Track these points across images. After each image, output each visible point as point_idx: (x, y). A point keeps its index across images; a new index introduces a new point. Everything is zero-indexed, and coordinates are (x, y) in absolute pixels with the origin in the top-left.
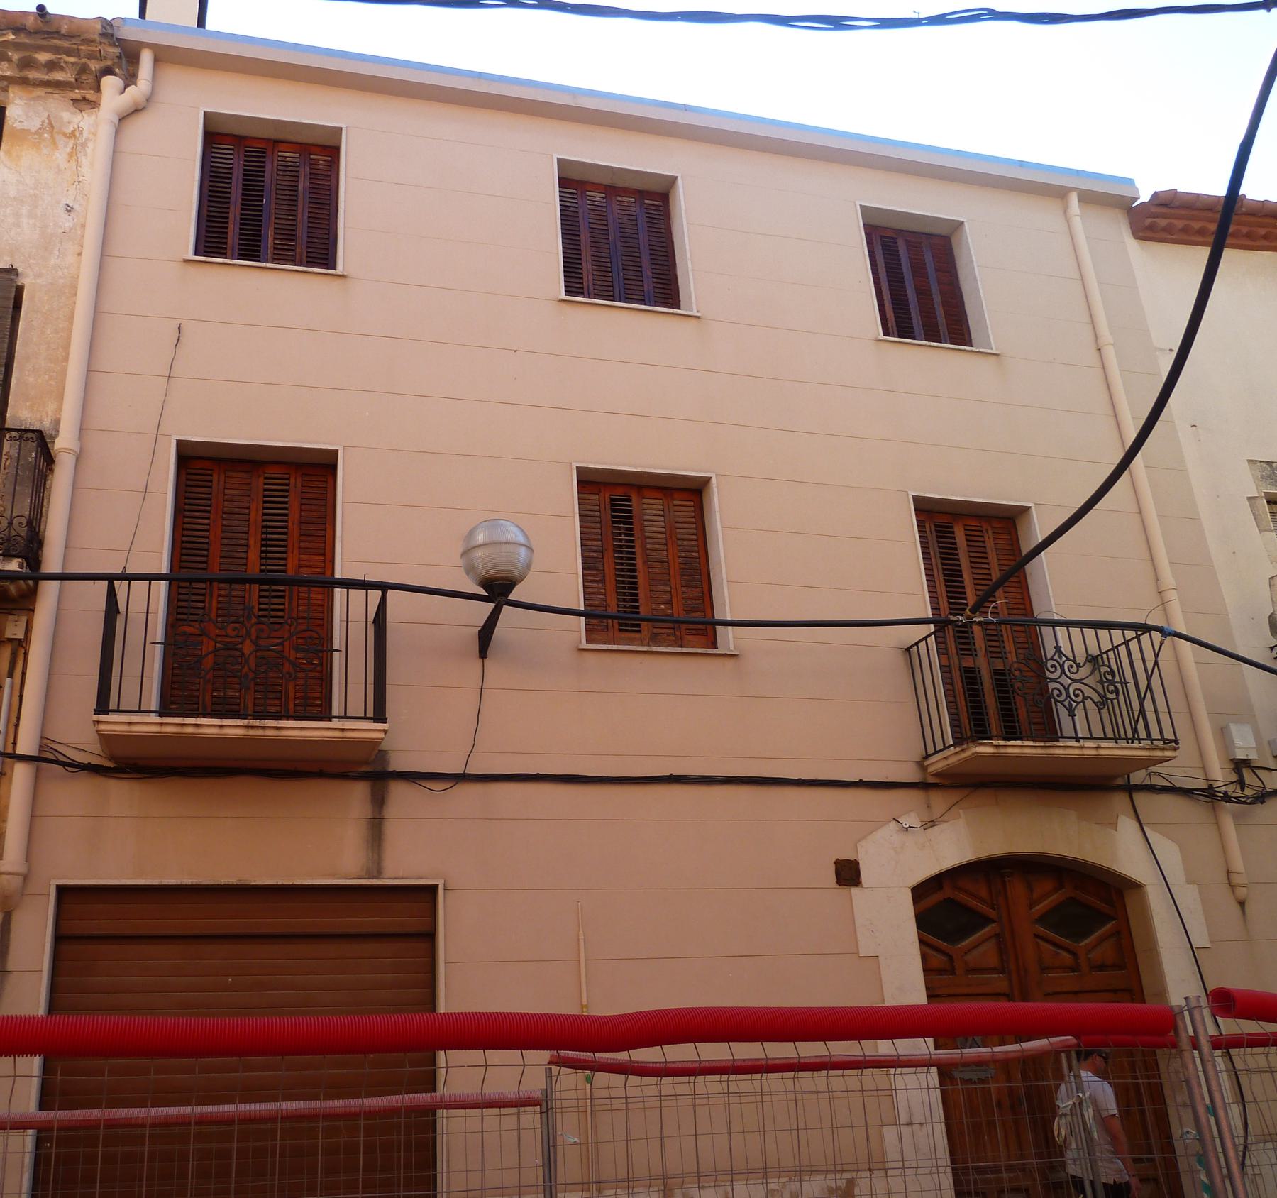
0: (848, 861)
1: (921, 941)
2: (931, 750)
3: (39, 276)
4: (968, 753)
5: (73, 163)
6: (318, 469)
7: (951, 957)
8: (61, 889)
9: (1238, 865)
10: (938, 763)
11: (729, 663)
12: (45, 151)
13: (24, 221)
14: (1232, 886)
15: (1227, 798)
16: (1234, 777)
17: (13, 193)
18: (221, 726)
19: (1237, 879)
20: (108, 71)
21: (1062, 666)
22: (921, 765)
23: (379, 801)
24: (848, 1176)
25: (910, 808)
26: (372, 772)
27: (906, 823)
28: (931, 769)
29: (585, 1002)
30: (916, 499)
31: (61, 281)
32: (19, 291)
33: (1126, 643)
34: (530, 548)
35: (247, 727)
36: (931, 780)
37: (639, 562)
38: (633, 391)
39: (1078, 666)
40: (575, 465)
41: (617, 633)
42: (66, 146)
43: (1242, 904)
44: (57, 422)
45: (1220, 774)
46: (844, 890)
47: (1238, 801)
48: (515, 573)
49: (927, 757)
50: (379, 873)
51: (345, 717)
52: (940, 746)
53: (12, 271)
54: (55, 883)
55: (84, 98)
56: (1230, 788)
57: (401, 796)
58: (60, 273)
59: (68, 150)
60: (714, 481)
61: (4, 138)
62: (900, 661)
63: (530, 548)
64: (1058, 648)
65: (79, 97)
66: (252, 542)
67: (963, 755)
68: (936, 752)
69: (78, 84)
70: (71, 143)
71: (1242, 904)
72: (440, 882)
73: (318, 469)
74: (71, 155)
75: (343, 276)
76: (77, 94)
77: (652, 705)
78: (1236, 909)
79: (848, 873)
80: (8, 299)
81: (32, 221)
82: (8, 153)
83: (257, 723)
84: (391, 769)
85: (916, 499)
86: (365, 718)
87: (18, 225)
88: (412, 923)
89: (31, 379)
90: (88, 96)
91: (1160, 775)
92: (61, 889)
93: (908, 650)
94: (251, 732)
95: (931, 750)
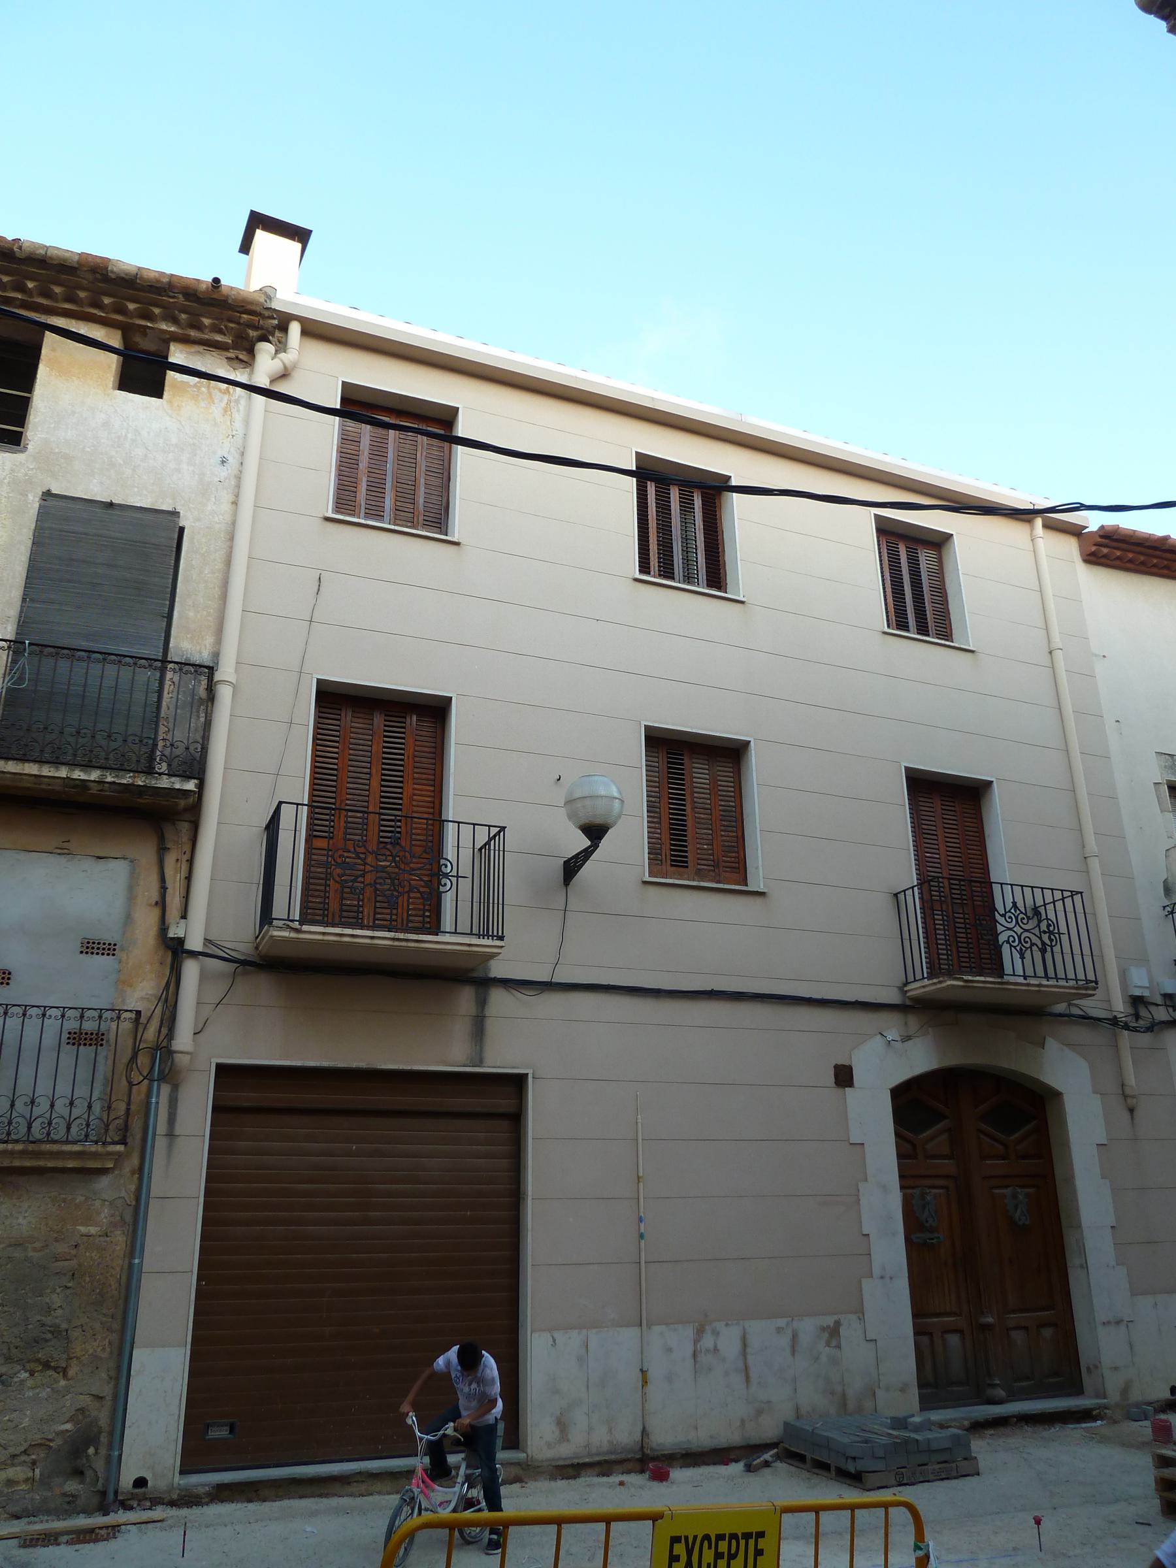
0: (844, 1066)
1: (897, 1134)
2: (911, 978)
3: (199, 520)
4: (944, 985)
5: (228, 418)
6: (434, 711)
7: (914, 1146)
8: (221, 1068)
9: (1131, 1080)
10: (916, 989)
11: (759, 901)
12: (203, 405)
13: (185, 467)
14: (1125, 1097)
15: (1126, 1027)
16: (1131, 1011)
17: (174, 441)
18: (372, 938)
19: (1128, 1091)
20: (264, 339)
21: (1017, 918)
22: (902, 989)
23: (482, 1003)
24: (835, 1317)
25: (893, 1026)
26: (468, 977)
27: (890, 1038)
28: (909, 994)
29: (641, 1174)
30: (907, 769)
31: (217, 526)
32: (182, 530)
33: (1063, 899)
34: (622, 801)
35: (393, 939)
36: (908, 1003)
37: (688, 808)
38: (685, 660)
39: (1029, 918)
40: (644, 723)
41: (669, 867)
42: (221, 401)
43: (1131, 1110)
44: (216, 655)
45: (1120, 1006)
46: (840, 1090)
47: (1135, 1030)
48: (609, 821)
49: (906, 983)
50: (481, 1063)
51: (456, 933)
52: (919, 976)
53: (175, 514)
54: (215, 1061)
55: (237, 358)
56: (1129, 1019)
57: (499, 999)
58: (216, 519)
59: (223, 405)
60: (752, 744)
61: (166, 388)
62: (889, 901)
63: (622, 801)
64: (1014, 904)
65: (233, 355)
66: (374, 771)
67: (939, 986)
68: (915, 980)
69: (235, 346)
70: (226, 398)
71: (1131, 1110)
72: (530, 1072)
73: (434, 711)
74: (225, 410)
75: (457, 544)
76: (231, 354)
77: (699, 931)
78: (1126, 1115)
79: (844, 1076)
80: (172, 539)
81: (191, 468)
82: (170, 402)
83: (401, 936)
84: (493, 975)
85: (907, 769)
86: (471, 934)
87: (178, 470)
88: (504, 1104)
89: (191, 614)
90: (241, 357)
91: (1077, 1006)
92: (221, 1068)
93: (896, 895)
94: (396, 943)
95: (911, 978)
